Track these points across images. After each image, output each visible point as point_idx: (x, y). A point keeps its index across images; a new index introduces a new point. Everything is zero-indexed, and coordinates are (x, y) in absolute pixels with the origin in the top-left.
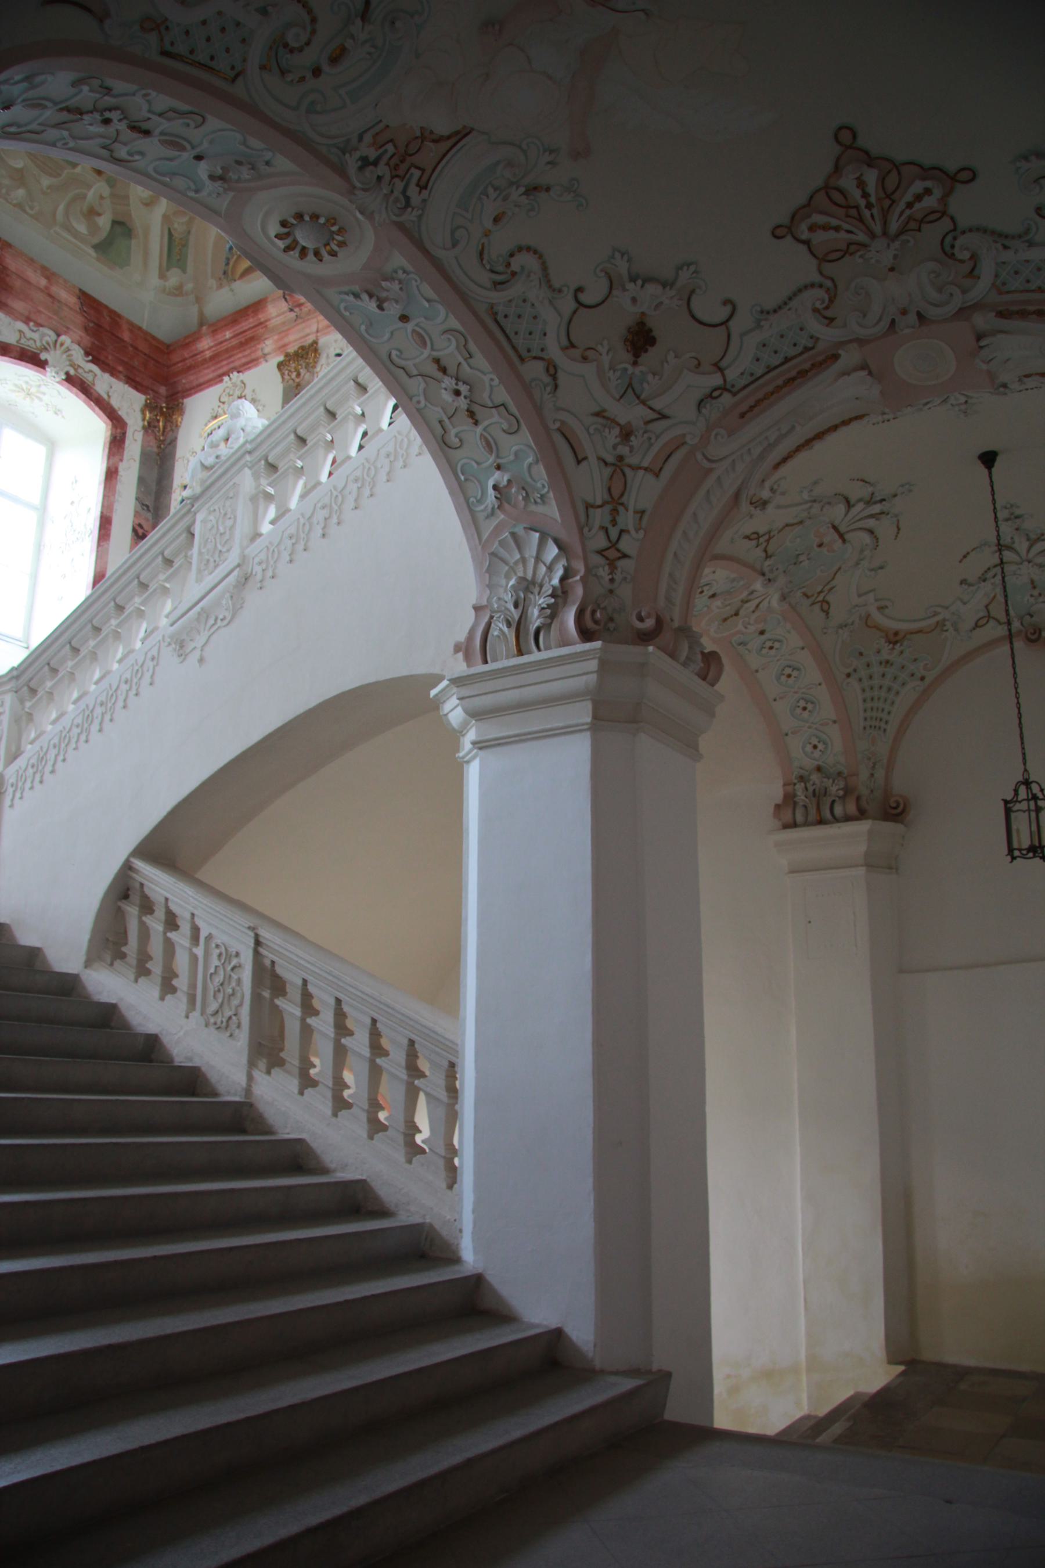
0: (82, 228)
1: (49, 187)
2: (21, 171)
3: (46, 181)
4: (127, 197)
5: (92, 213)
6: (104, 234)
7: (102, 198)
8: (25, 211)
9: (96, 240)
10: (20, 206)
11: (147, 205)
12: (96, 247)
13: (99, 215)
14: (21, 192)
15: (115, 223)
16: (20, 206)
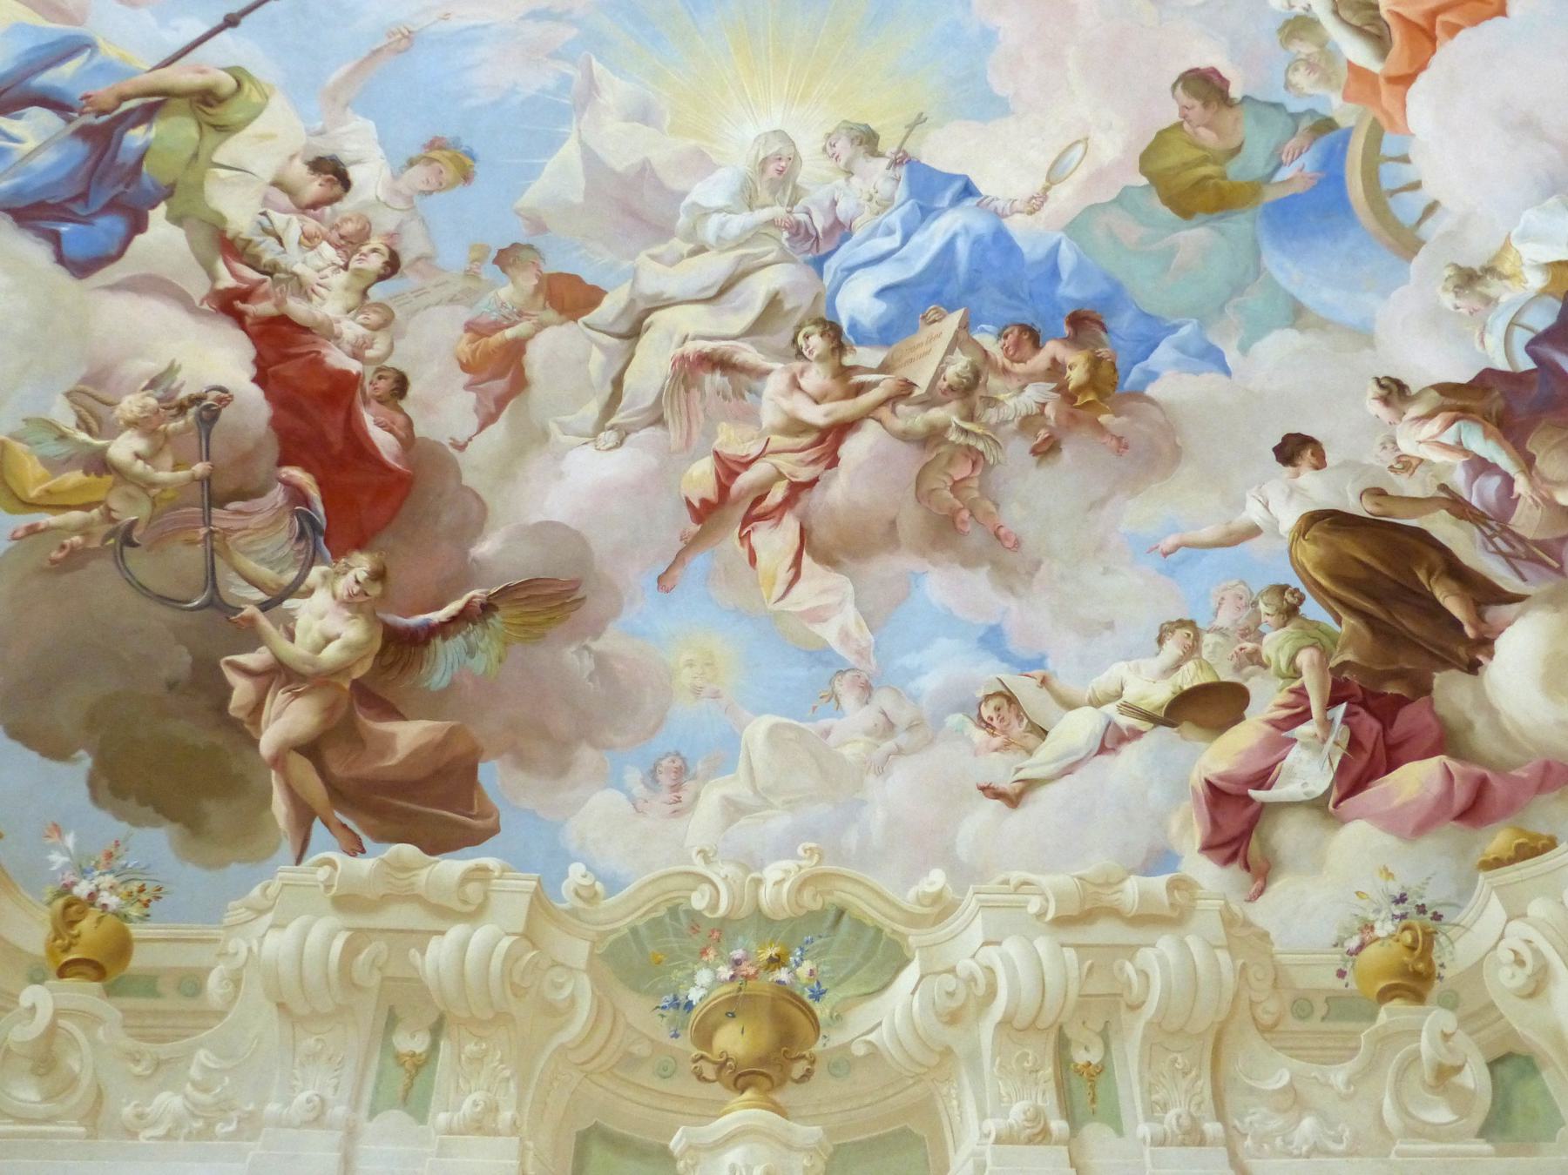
0: (1441, 1114)
1: (1349, 1083)
2: (1290, 1088)
3: (1339, 1076)
4: (1491, 1006)
5: (1444, 1074)
6: (1485, 1101)
7: (1446, 1037)
8: (1328, 1153)
9: (1477, 1120)
10: (1316, 1150)
11: (1531, 995)
12: (1484, 1132)
13: (1458, 1069)
14: (1308, 1123)
15: (1493, 1065)
16: (1316, 1150)
